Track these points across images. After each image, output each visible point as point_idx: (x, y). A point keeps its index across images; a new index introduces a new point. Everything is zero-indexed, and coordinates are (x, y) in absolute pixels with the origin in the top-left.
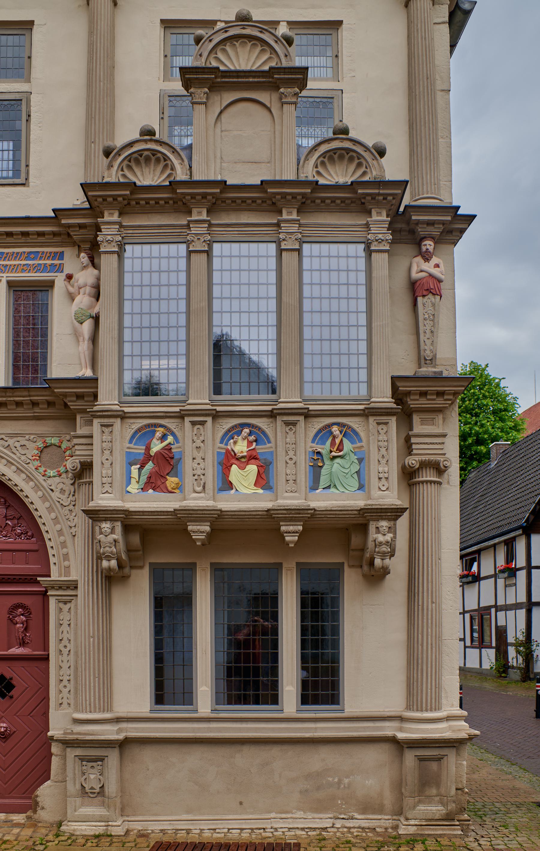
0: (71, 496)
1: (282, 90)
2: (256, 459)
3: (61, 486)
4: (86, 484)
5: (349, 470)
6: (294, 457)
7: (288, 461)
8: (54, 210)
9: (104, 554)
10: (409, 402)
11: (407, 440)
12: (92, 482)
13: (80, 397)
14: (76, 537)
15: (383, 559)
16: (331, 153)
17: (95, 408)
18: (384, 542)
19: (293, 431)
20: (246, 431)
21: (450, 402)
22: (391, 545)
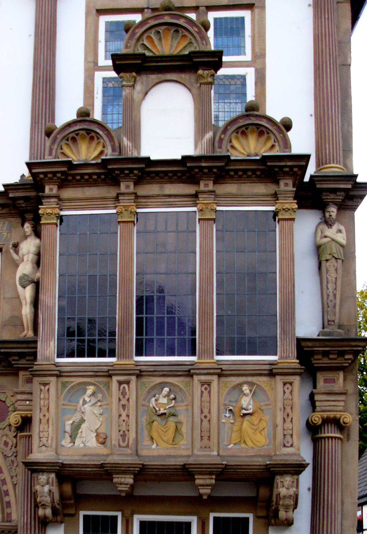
0: (13, 447)
1: (200, 72)
2: (175, 416)
3: (4, 439)
4: (26, 437)
5: (258, 426)
6: (208, 415)
7: (203, 418)
8: (4, 186)
9: (40, 503)
10: (313, 362)
11: (312, 397)
12: (31, 435)
13: (22, 356)
14: (17, 486)
15: (286, 512)
16: (244, 129)
17: (35, 368)
18: (288, 496)
19: (208, 390)
20: (166, 389)
21: (350, 361)
22: (296, 498)
